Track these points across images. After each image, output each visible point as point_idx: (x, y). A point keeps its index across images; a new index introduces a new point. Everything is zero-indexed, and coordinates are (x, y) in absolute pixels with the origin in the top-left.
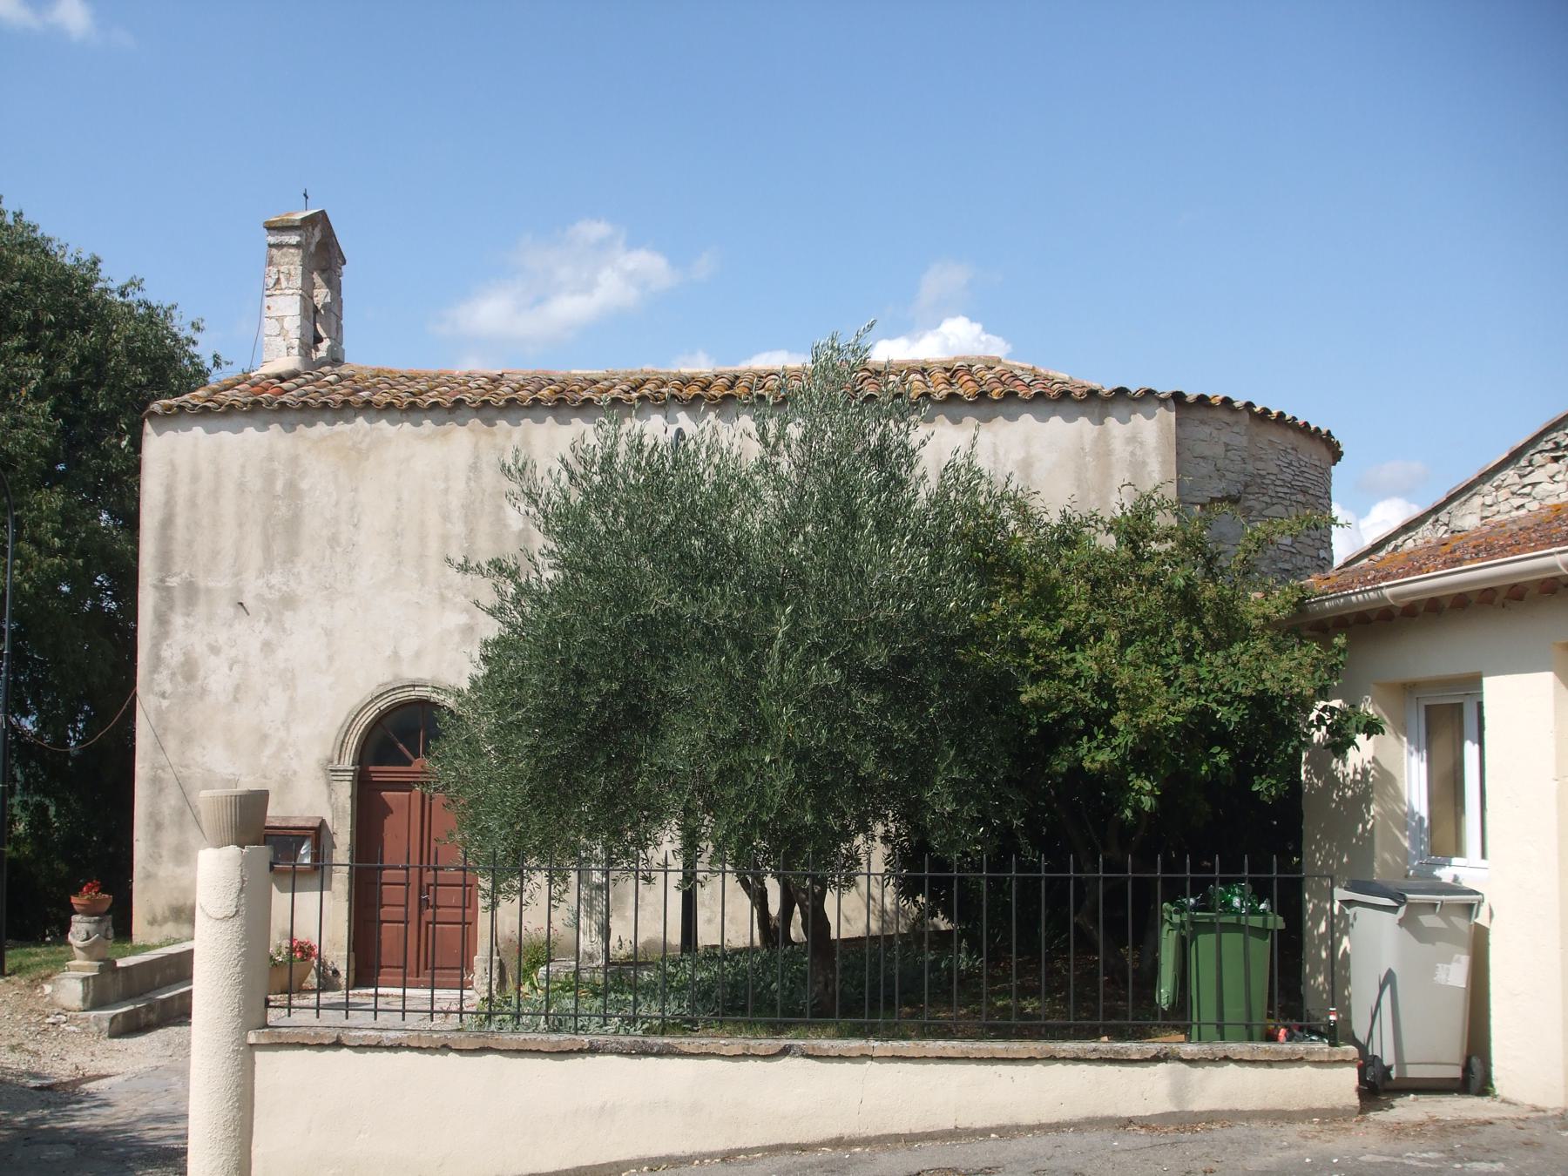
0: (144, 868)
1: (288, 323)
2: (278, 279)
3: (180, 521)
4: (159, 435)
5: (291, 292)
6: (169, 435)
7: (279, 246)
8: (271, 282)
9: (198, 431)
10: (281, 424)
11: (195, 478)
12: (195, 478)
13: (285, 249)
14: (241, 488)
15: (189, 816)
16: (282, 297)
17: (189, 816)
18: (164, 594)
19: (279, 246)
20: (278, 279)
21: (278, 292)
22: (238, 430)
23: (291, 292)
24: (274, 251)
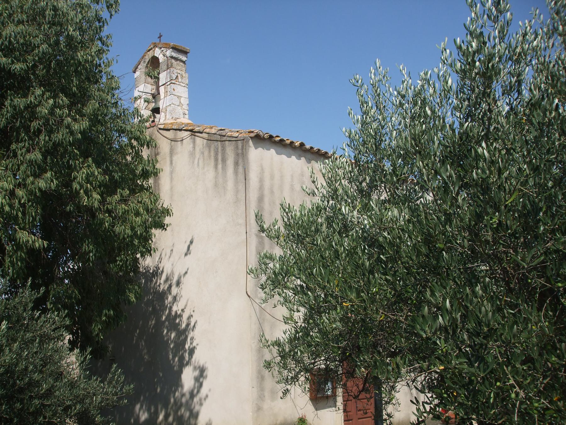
0: (257, 404)
1: (183, 100)
2: (177, 76)
3: (266, 200)
4: (256, 148)
5: (184, 85)
6: (260, 149)
7: (176, 59)
8: (174, 77)
9: (273, 151)
10: (305, 158)
11: (272, 177)
12: (272, 177)
13: (178, 62)
14: (292, 188)
15: (415, 402)
16: (180, 86)
17: (415, 402)
18: (260, 240)
19: (176, 59)
20: (177, 76)
21: (177, 83)
22: (289, 156)
23: (184, 85)
24: (173, 61)
